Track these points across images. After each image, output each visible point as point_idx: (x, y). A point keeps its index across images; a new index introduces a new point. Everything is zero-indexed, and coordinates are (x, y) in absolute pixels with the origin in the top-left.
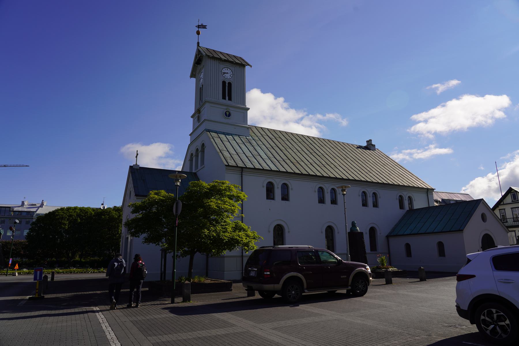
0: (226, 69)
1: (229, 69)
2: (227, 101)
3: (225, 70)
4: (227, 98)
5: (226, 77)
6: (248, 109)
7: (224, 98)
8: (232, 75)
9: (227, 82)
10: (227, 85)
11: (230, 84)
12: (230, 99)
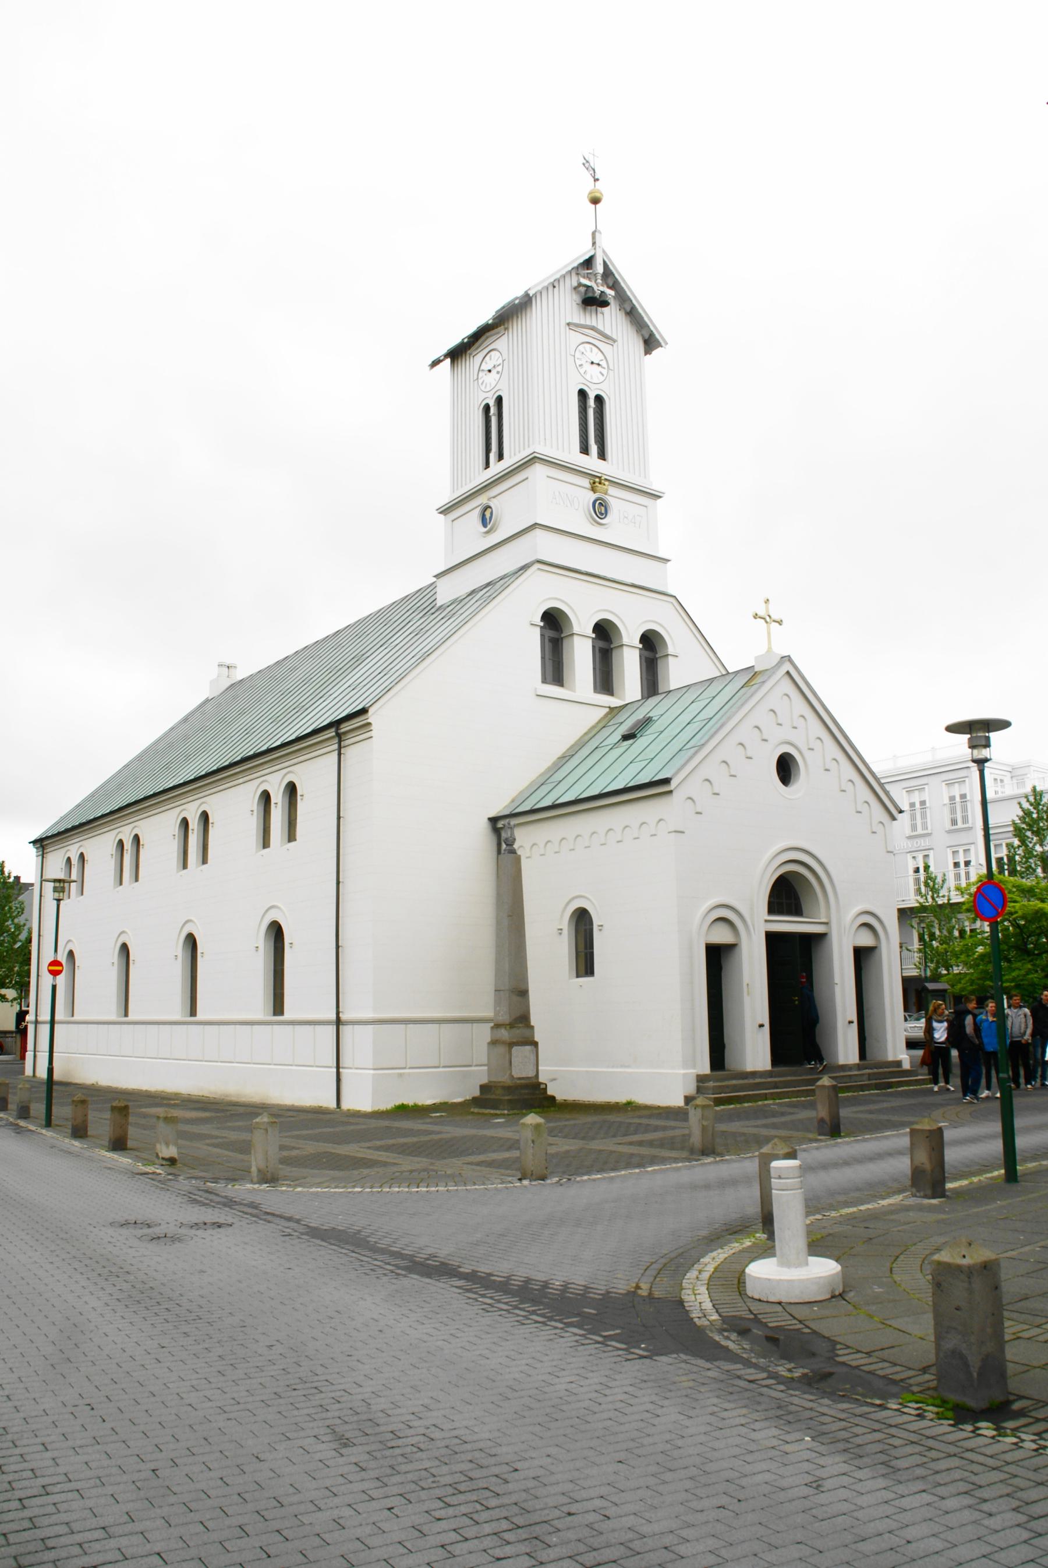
0: (588, 346)
2: (591, 462)
4: (594, 448)
5: (588, 377)
7: (585, 450)
9: (592, 396)
10: (591, 403)
11: (599, 399)
12: (602, 455)
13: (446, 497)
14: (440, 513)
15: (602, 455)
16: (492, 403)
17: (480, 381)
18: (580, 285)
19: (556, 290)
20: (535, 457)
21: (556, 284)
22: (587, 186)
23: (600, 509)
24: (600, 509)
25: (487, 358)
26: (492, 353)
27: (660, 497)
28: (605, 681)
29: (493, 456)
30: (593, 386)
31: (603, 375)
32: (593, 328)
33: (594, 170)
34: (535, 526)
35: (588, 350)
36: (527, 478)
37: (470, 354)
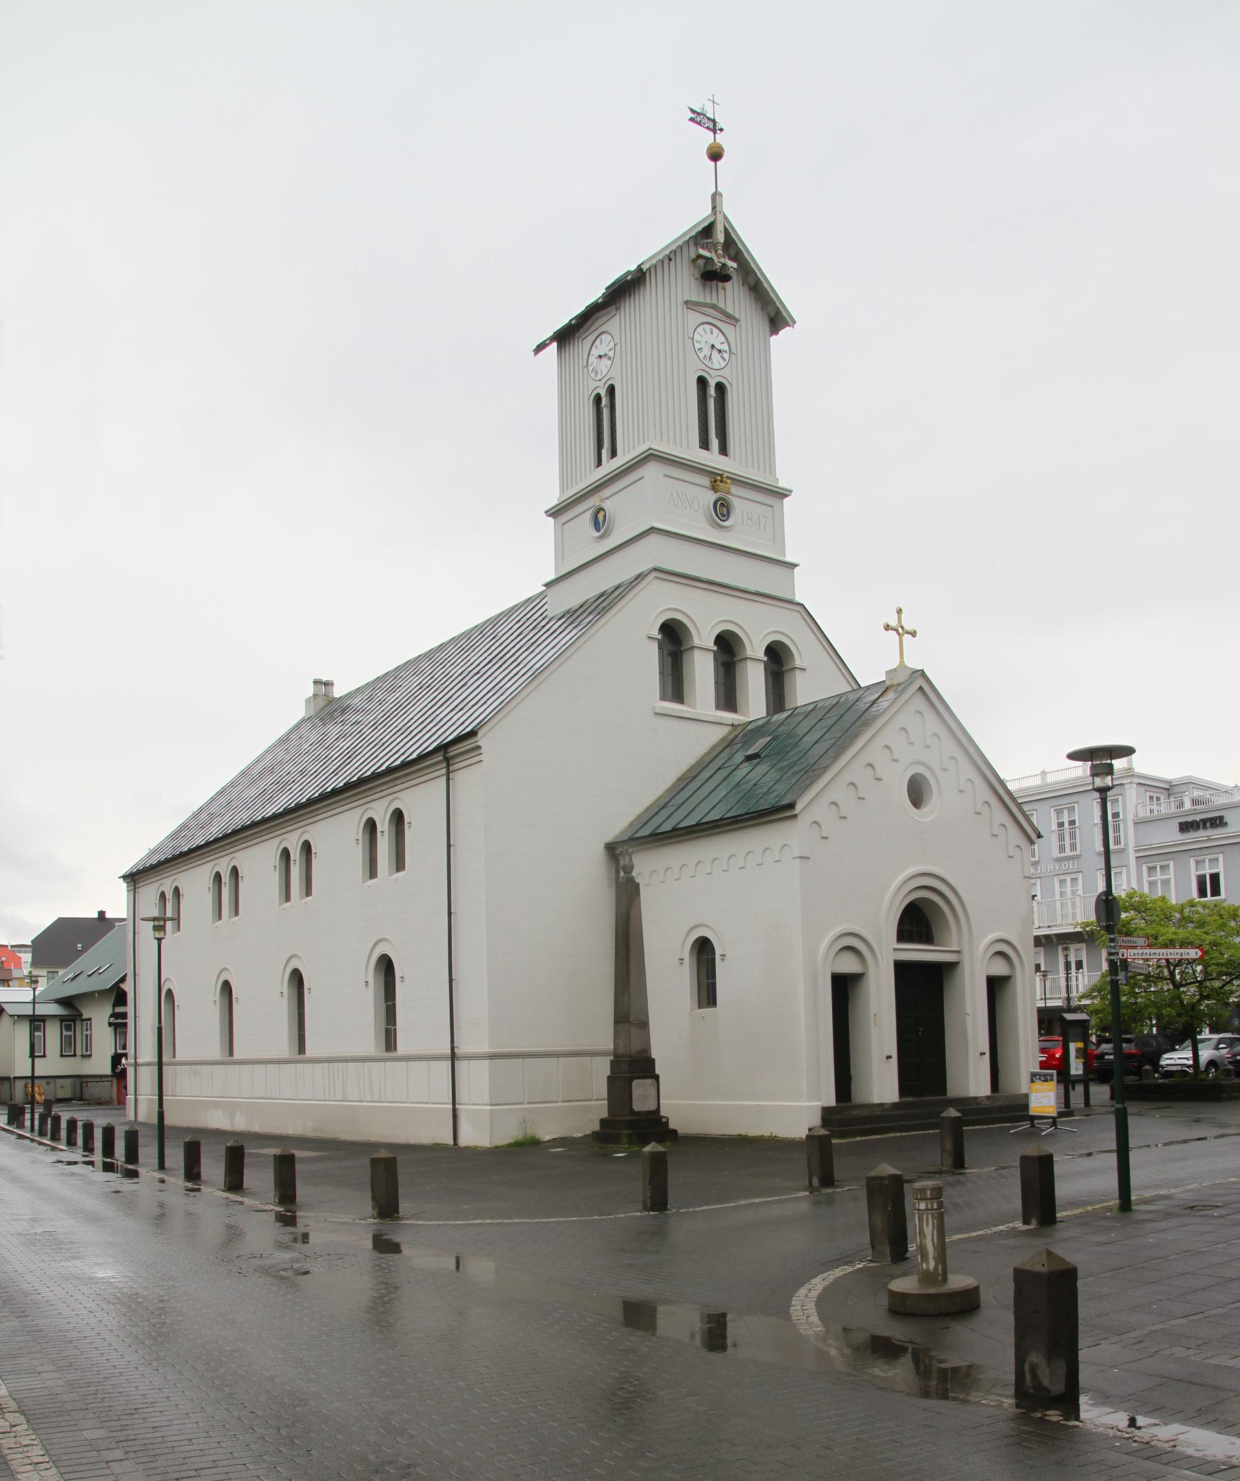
0: (707, 327)
1: (716, 331)
2: (712, 458)
3: (706, 333)
4: (714, 443)
6: (782, 494)
7: (705, 445)
8: (726, 356)
10: (712, 391)
11: (720, 388)
12: (724, 450)
13: (554, 500)
14: (550, 516)
15: (724, 450)
16: (603, 393)
17: (590, 368)
18: (699, 256)
19: (672, 263)
20: (651, 454)
21: (672, 256)
22: (706, 138)
23: (722, 509)
24: (722, 509)
25: (598, 342)
26: (604, 336)
27: (787, 496)
28: (728, 697)
29: (605, 453)
30: (713, 373)
31: (725, 360)
32: (714, 307)
33: (714, 121)
34: (653, 530)
35: (708, 331)
36: (643, 477)
37: (578, 338)
